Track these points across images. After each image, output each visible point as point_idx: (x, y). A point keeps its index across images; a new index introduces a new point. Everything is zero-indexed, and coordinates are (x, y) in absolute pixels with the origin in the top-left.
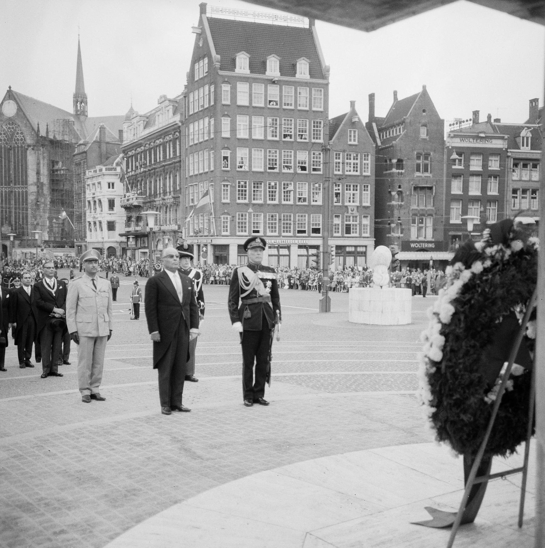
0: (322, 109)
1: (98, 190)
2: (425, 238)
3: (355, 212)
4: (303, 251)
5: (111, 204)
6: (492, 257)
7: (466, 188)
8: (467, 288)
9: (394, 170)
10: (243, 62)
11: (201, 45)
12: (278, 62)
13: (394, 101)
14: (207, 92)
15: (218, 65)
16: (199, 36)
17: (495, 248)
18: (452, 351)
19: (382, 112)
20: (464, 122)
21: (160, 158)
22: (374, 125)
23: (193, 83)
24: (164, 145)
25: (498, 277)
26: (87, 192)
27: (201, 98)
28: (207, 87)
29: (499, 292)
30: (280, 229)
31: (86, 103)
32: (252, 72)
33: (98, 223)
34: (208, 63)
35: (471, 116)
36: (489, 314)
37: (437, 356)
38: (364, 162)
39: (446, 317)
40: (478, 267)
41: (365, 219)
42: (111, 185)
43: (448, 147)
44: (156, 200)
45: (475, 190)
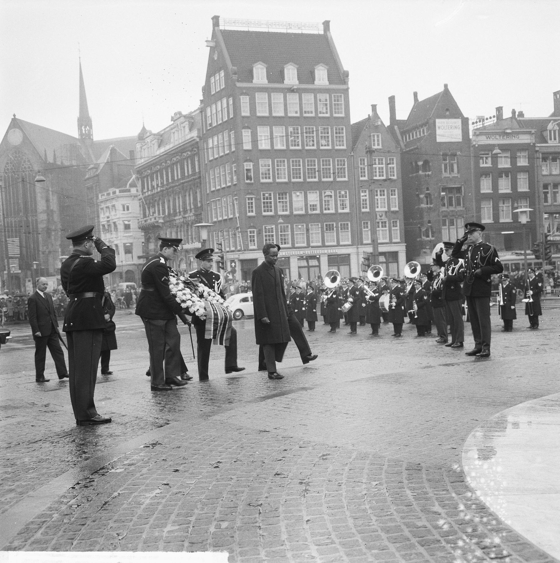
0: (343, 115)
3: (384, 219)
11: (216, 59)
13: (415, 103)
14: (225, 105)
16: (212, 50)
19: (403, 114)
20: (487, 119)
21: (178, 176)
22: (396, 127)
23: (209, 97)
26: (102, 216)
27: (219, 112)
28: (225, 101)
31: (91, 127)
34: (225, 76)
35: (494, 113)
44: (175, 218)
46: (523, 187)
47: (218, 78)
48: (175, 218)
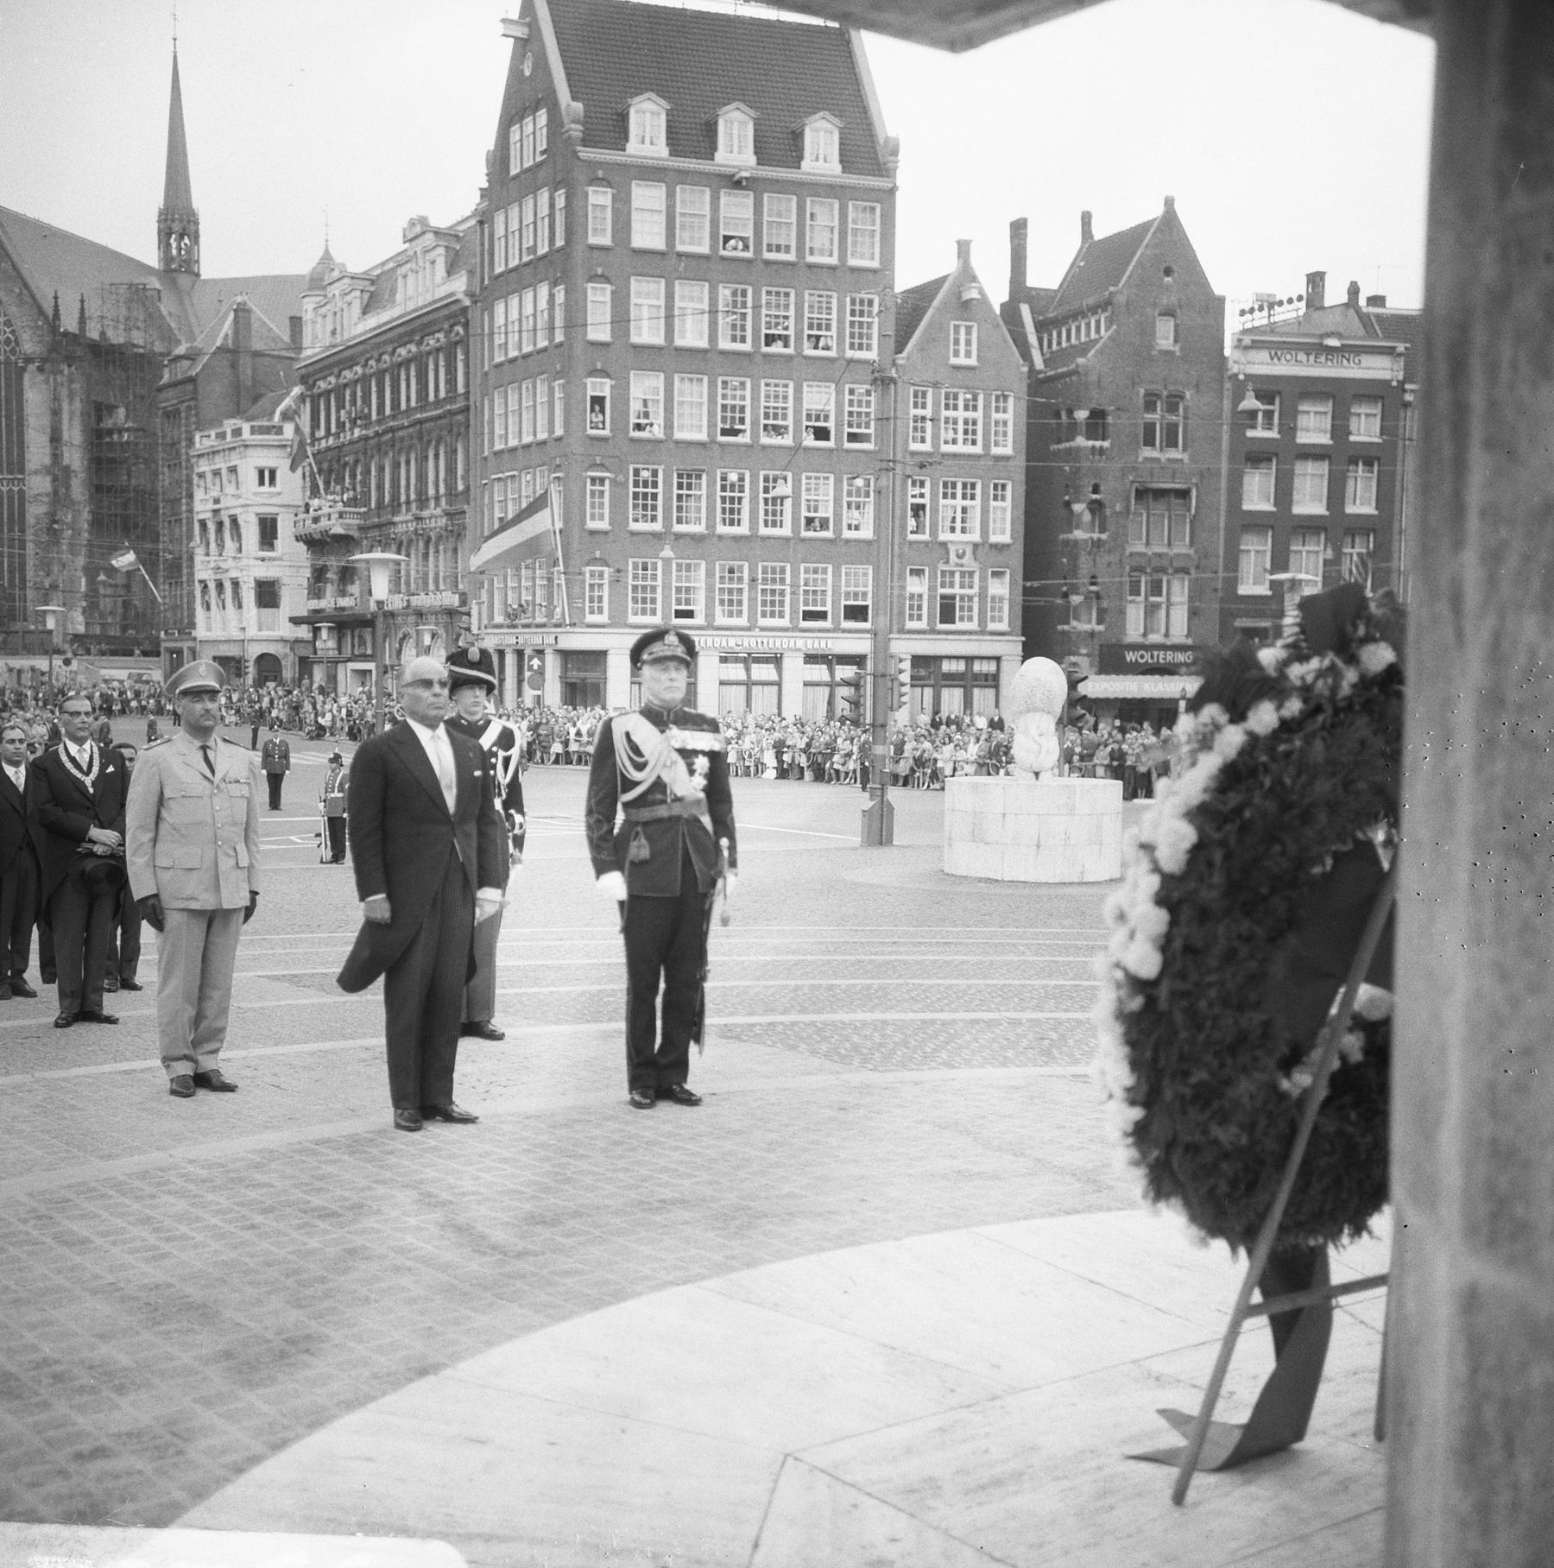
0: (875, 264)
1: (230, 489)
2: (1167, 635)
3: (968, 559)
4: (820, 672)
5: (268, 531)
6: (1306, 691)
7: (1284, 494)
8: (1232, 776)
9: (1081, 441)
10: (648, 123)
11: (527, 73)
12: (751, 127)
14: (544, 210)
15: (576, 131)
17: (1315, 663)
18: (1188, 949)
19: (1049, 270)
20: (1280, 303)
21: (408, 400)
22: (1025, 310)
23: (504, 185)
24: (420, 361)
25: (1318, 745)
26: (199, 494)
27: (528, 228)
28: (544, 196)
29: (1323, 787)
30: (752, 610)
31: (196, 238)
32: (674, 152)
33: (228, 586)
35: (1302, 288)
36: (1293, 849)
37: (1146, 962)
38: (995, 416)
39: (1172, 856)
40: (1264, 717)
41: (916, 578)
42: (267, 476)
43: (1236, 375)
44: (396, 519)
45: (1309, 502)
46: (1362, 502)
47: (529, 128)
48: (396, 519)
